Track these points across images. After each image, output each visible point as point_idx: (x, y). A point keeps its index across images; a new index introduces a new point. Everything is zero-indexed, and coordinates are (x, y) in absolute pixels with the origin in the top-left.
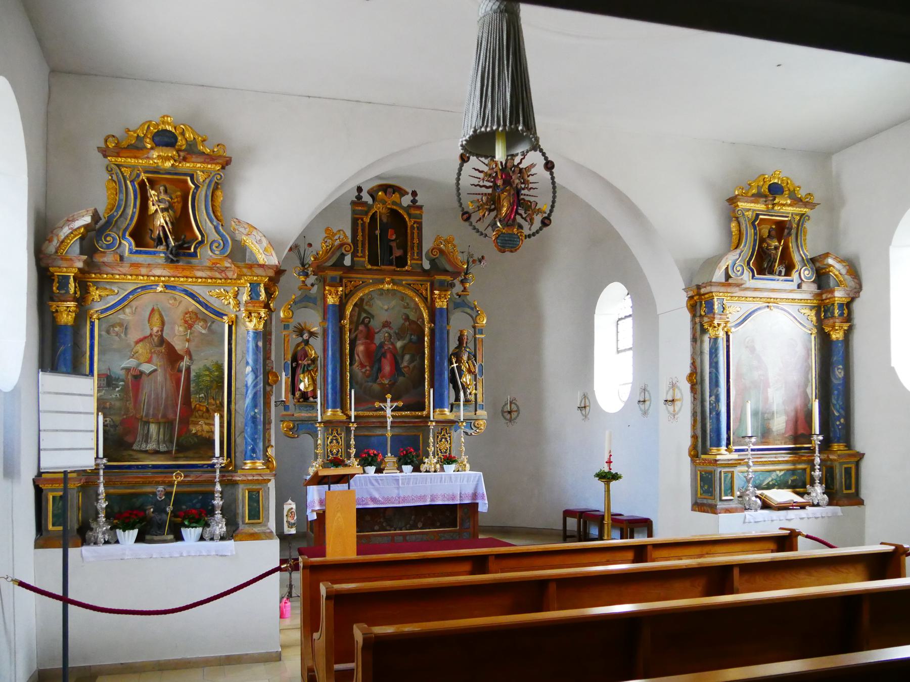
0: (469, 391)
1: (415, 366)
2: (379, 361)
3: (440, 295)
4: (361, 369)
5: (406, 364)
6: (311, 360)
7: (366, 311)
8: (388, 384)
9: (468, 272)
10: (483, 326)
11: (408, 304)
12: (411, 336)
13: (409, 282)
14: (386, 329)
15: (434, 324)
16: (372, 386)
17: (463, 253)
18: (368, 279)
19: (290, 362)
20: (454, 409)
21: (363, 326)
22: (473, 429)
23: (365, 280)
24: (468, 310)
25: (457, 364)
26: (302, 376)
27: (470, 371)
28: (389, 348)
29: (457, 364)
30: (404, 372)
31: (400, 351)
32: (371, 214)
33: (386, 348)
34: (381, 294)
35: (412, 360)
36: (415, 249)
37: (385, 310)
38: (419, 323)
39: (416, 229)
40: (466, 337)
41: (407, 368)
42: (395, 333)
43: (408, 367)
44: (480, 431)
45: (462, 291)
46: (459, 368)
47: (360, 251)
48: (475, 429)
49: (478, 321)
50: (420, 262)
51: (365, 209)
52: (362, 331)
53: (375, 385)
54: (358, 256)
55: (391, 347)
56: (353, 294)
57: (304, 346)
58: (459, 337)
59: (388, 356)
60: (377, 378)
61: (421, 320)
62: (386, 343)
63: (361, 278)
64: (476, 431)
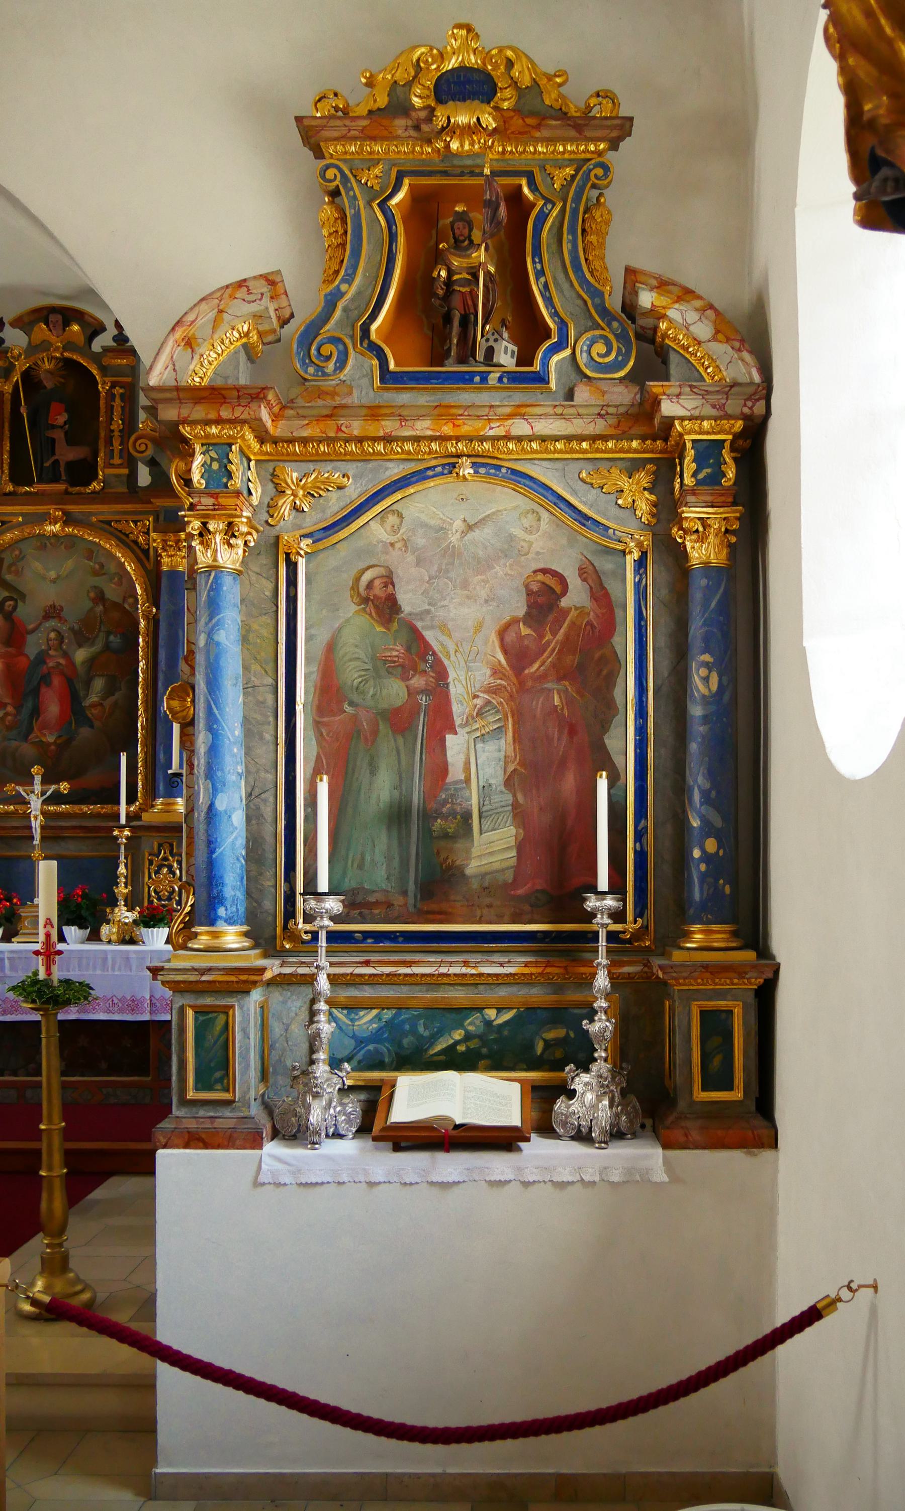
2: (36, 692)
5: (95, 699)
11: (102, 566)
13: (102, 518)
14: (52, 623)
28: (59, 664)
30: (90, 716)
33: (51, 664)
34: (43, 547)
35: (110, 690)
38: (126, 606)
41: (99, 708)
42: (72, 629)
55: (62, 661)
59: (56, 681)
60: (30, 730)
61: (131, 600)
62: (51, 652)
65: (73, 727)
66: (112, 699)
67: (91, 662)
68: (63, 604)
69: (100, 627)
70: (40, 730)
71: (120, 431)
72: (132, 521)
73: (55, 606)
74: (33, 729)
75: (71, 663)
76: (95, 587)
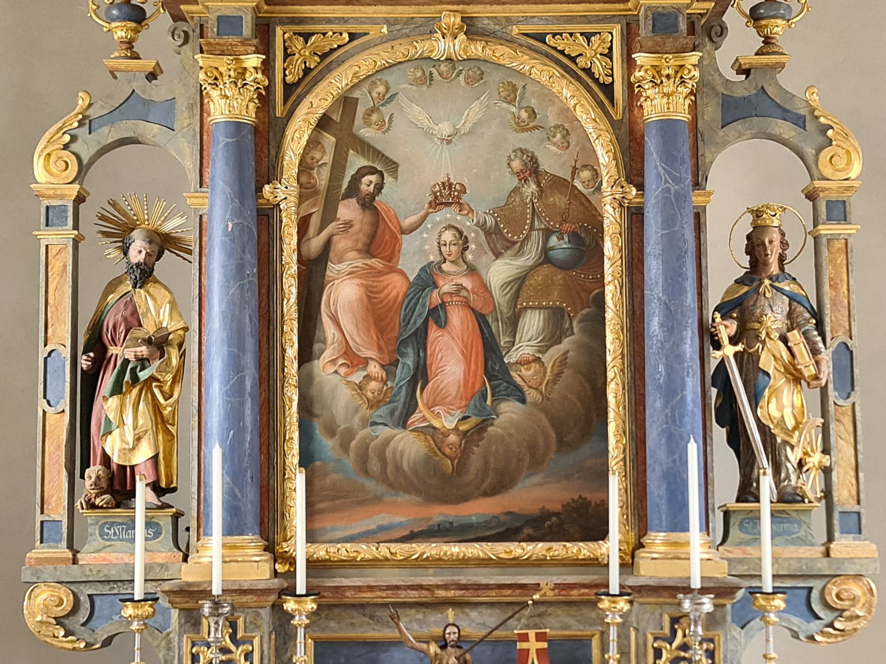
0: (794, 456)
1: (563, 360)
2: (420, 338)
3: (657, 69)
4: (347, 375)
6: (148, 342)
7: (366, 148)
8: (456, 429)
11: (533, 114)
14: (447, 214)
15: (640, 187)
16: (387, 442)
18: (373, 21)
19: (66, 353)
20: (734, 532)
22: (818, 618)
25: (740, 347)
26: (114, 402)
27: (795, 377)
28: (460, 287)
29: (740, 347)
30: (518, 380)
31: (501, 298)
33: (446, 288)
38: (578, 184)
40: (776, 237)
41: (535, 366)
42: (482, 226)
43: (537, 360)
44: (849, 626)
45: (756, 54)
49: (827, 171)
52: (348, 224)
53: (407, 432)
55: (467, 282)
56: (315, 83)
57: (130, 288)
58: (749, 237)
59: (457, 317)
60: (411, 407)
61: (586, 174)
63: (345, 21)
64: (831, 625)
65: (489, 402)
66: (556, 351)
67: (519, 283)
68: (465, 182)
72: (582, 34)
73: (450, 185)
76: (522, 151)
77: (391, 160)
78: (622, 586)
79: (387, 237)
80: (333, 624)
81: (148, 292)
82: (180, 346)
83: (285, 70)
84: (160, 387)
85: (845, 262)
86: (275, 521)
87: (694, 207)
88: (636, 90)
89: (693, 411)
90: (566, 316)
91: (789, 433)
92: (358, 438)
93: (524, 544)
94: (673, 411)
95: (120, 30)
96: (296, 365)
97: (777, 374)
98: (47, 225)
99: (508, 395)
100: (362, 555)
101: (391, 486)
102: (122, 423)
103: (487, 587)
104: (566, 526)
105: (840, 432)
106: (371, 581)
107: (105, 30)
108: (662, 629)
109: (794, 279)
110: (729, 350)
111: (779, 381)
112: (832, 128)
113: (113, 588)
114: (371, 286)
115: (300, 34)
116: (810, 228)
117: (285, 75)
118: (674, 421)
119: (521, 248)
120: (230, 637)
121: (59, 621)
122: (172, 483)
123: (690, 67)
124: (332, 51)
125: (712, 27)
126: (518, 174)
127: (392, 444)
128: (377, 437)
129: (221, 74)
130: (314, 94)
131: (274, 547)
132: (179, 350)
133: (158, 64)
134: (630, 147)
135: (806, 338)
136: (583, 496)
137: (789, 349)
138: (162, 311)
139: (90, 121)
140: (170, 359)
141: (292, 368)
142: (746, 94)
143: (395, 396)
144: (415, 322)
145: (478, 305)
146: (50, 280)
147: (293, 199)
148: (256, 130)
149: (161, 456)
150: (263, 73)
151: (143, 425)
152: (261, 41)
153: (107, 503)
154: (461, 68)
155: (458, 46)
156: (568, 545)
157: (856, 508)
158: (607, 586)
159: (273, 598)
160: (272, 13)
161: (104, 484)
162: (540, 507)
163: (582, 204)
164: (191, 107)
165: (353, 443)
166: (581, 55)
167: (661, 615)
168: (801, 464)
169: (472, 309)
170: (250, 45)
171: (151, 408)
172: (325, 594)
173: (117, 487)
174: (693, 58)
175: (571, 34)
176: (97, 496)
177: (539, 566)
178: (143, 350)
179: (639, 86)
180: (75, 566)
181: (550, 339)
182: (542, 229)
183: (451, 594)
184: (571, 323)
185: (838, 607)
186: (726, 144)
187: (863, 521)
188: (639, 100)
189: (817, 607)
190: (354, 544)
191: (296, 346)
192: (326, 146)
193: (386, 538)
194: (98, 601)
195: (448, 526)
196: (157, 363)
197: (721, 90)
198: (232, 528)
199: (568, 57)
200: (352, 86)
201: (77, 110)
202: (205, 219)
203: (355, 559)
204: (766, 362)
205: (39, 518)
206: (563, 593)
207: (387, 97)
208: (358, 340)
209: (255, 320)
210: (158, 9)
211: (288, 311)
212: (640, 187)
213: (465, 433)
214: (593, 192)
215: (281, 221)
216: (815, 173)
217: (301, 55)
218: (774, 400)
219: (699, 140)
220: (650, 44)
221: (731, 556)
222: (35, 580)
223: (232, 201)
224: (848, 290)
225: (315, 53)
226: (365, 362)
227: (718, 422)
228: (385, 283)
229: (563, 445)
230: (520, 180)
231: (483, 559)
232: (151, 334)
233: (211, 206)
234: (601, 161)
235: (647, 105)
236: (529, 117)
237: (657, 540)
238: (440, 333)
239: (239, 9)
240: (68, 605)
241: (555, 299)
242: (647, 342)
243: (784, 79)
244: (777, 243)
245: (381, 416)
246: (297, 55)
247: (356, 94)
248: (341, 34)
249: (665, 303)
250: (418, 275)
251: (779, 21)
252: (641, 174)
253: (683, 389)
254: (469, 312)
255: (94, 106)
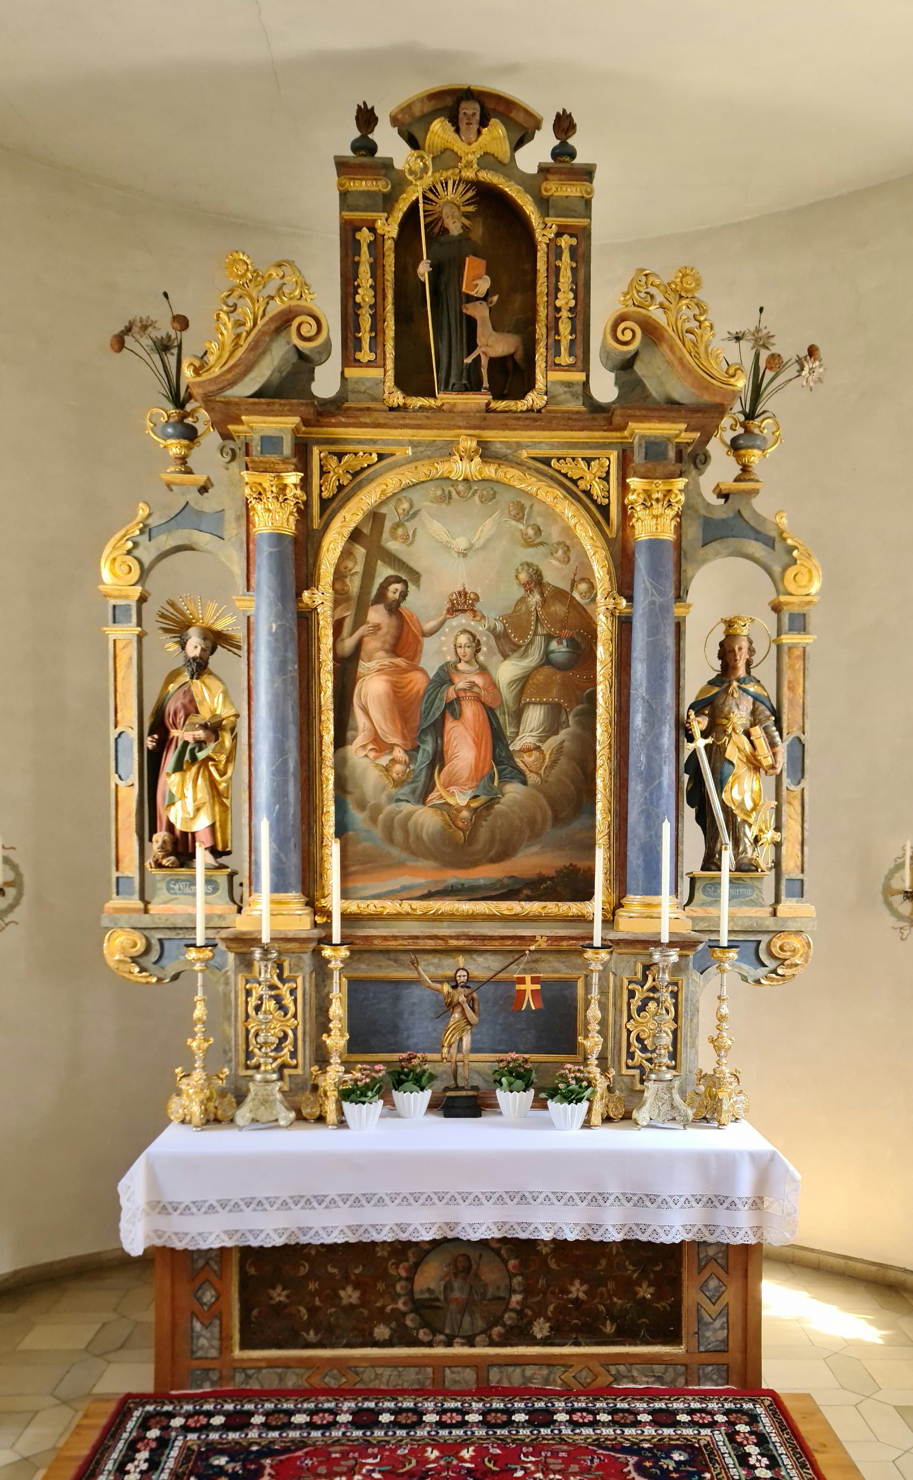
0: (750, 833)
1: (560, 747)
2: (438, 729)
3: (648, 493)
4: (376, 758)
6: (205, 727)
7: (392, 559)
8: (468, 806)
9: (759, 410)
10: (809, 603)
11: (538, 531)
12: (547, 645)
14: (462, 620)
15: (630, 599)
16: (409, 816)
17: (738, 339)
18: (399, 443)
19: (134, 734)
20: (699, 896)
21: (381, 607)
22: (764, 965)
23: (385, 450)
24: (756, 548)
25: (710, 740)
26: (176, 778)
27: (755, 765)
28: (473, 684)
29: (710, 740)
30: (521, 765)
31: (507, 694)
32: (402, 207)
35: (552, 727)
36: (561, 327)
37: (459, 553)
38: (576, 595)
39: (566, 256)
40: (745, 644)
41: (535, 754)
42: (493, 630)
46: (716, 753)
47: (366, 345)
48: (771, 964)
49: (791, 587)
50: (580, 377)
51: (381, 186)
52: (377, 627)
53: (426, 809)
54: (358, 363)
56: (348, 499)
57: (188, 679)
59: (470, 710)
60: (430, 787)
61: (583, 587)
62: (462, 666)
63: (374, 442)
64: (774, 971)
65: (496, 784)
66: (553, 741)
67: (523, 682)
68: (479, 592)
69: (536, 627)
70: (446, 786)
71: (571, 310)
72: (583, 459)
73: (466, 594)
74: (434, 785)
75: (493, 685)
76: (529, 565)
77: (414, 571)
78: (603, 939)
79: (410, 640)
80: (363, 966)
81: (204, 683)
82: (232, 730)
83: (321, 486)
84: (216, 766)
85: (802, 667)
86: (315, 881)
87: (676, 617)
88: (629, 512)
89: (668, 794)
90: (563, 711)
91: (748, 813)
92: (385, 812)
93: (523, 903)
94: (651, 794)
95: (175, 448)
96: (332, 749)
97: (740, 764)
98: (114, 622)
99: (512, 778)
100: (388, 910)
101: (413, 853)
102: (183, 796)
103: (492, 938)
104: (559, 889)
105: (790, 813)
106: (395, 932)
107: (162, 446)
108: (635, 974)
109: (758, 681)
110: (701, 743)
111: (741, 768)
112: (796, 548)
113: (178, 934)
114: (397, 682)
115: (335, 454)
116: (774, 637)
117: (321, 491)
118: (652, 803)
119: (526, 651)
120: (278, 976)
121: (134, 960)
122: (227, 847)
123: (677, 492)
124: (363, 469)
125: (698, 455)
126: (524, 585)
127: (414, 819)
128: (401, 811)
129: (265, 490)
130: (347, 509)
131: (314, 903)
132: (232, 734)
133: (209, 479)
134: (622, 563)
135: (766, 733)
136: (574, 863)
137: (752, 742)
138: (216, 700)
139: (150, 530)
140: (223, 741)
141: (329, 751)
142: (724, 516)
143: (417, 777)
144: (434, 714)
145: (488, 699)
146: (118, 670)
147: (329, 604)
148: (296, 540)
149: (218, 824)
150: (302, 489)
151: (201, 798)
152: (300, 460)
153: (172, 864)
154: (476, 488)
155: (474, 468)
156: (560, 904)
157: (800, 876)
158: (592, 939)
159: (313, 945)
160: (310, 433)
161: (169, 848)
162: (538, 872)
163: (579, 613)
164: (238, 519)
165: (381, 817)
166: (582, 478)
167: (635, 963)
168: (756, 840)
169: (484, 704)
170: (290, 463)
171: (208, 783)
172: (357, 942)
173: (180, 849)
174: (680, 483)
175: (574, 459)
176: (164, 857)
177: (535, 921)
178: (201, 734)
179: (632, 508)
180: (147, 915)
181: (548, 731)
182: (544, 635)
183: (461, 943)
184: (567, 718)
185: (781, 957)
186: (704, 561)
187: (805, 888)
188: (631, 520)
189: (763, 957)
190: (381, 901)
191: (332, 732)
192: (357, 556)
193: (409, 896)
194: (167, 944)
195: (460, 887)
196: (212, 745)
197: (703, 512)
198: (279, 887)
199: (571, 479)
200: (381, 503)
201: (138, 519)
202: (252, 620)
203: (381, 914)
204: (731, 753)
205: (115, 874)
206: (555, 943)
207: (411, 513)
208: (384, 727)
209: (297, 710)
210: (209, 428)
211: (325, 702)
212: (630, 599)
213: (477, 809)
214: (589, 603)
215: (319, 624)
216: (781, 588)
217: (335, 473)
218: (736, 786)
219: (682, 557)
220: (642, 470)
221: (695, 914)
222: (112, 925)
223: (276, 605)
224: (804, 691)
225: (348, 472)
226: (391, 747)
227: (689, 803)
228: (408, 680)
229: (558, 820)
230: (526, 591)
231: (489, 915)
232: (207, 719)
233: (258, 608)
234: (597, 575)
235: (638, 526)
236: (535, 534)
237: (634, 901)
238: (455, 723)
239: (281, 430)
240: (141, 946)
241: (554, 696)
242: (632, 735)
243: (760, 505)
244: (745, 650)
245: (404, 794)
246: (332, 474)
247: (384, 510)
248: (371, 454)
249: (648, 702)
250: (437, 673)
251: (756, 451)
252: (631, 587)
253: (660, 776)
254: (479, 706)
255: (153, 516)
